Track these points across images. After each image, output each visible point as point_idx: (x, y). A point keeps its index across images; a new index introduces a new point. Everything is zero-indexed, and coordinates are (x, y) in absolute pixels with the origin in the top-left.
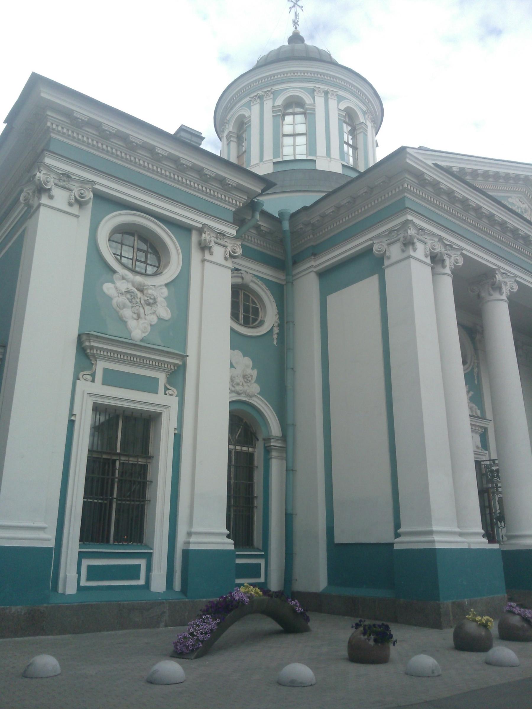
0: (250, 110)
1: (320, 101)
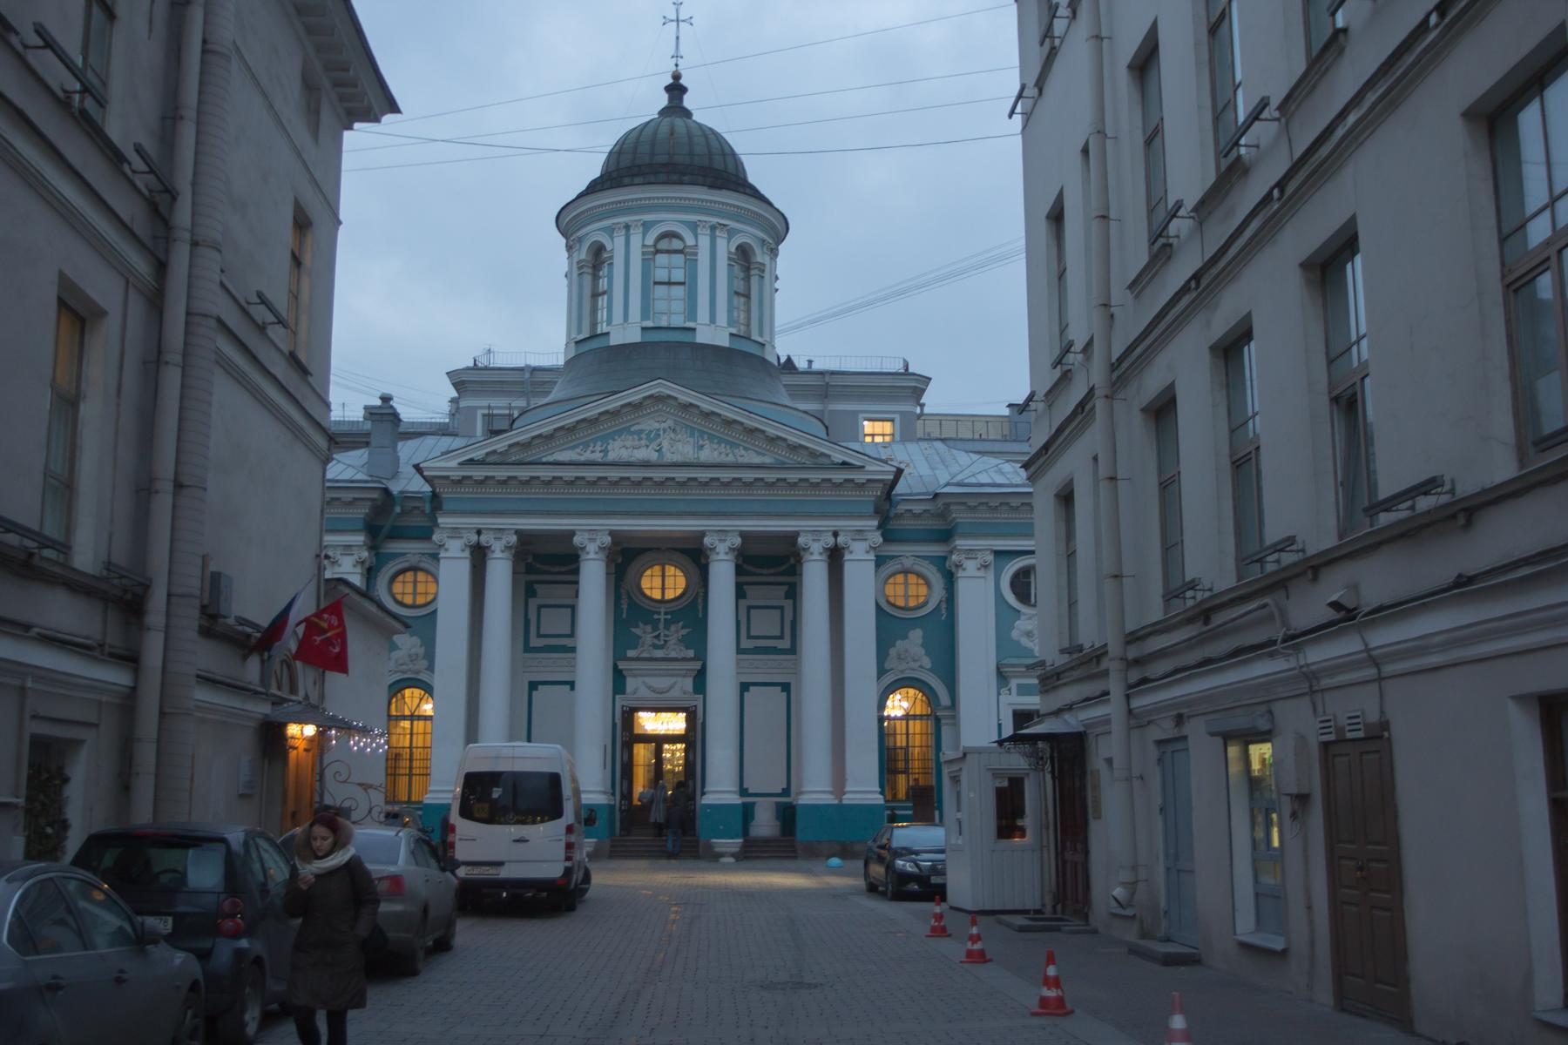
0: (612, 240)
1: (704, 241)
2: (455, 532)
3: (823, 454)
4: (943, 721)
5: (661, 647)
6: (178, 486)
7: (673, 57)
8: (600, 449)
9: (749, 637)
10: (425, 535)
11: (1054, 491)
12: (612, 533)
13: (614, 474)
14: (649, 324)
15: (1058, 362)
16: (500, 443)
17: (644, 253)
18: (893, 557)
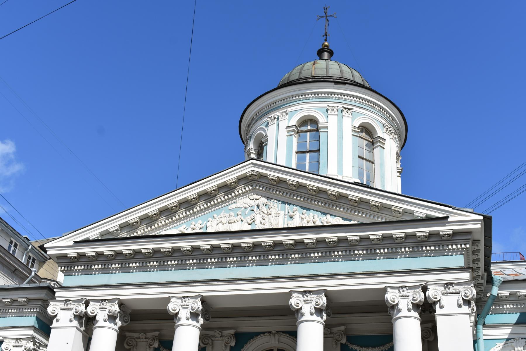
3: (405, 211)
7: (323, 36)
8: (200, 226)
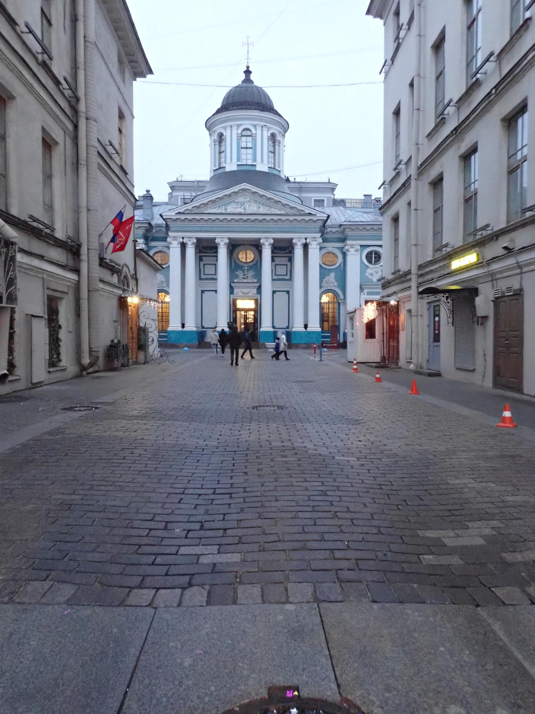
1: (259, 132)
2: (175, 238)
3: (302, 210)
4: (341, 304)
5: (246, 278)
6: (88, 210)
9: (276, 275)
10: (164, 239)
11: (391, 217)
12: (229, 238)
13: (229, 217)
14: (240, 163)
15: (395, 169)
16: (189, 207)
17: (237, 136)
18: (325, 247)
